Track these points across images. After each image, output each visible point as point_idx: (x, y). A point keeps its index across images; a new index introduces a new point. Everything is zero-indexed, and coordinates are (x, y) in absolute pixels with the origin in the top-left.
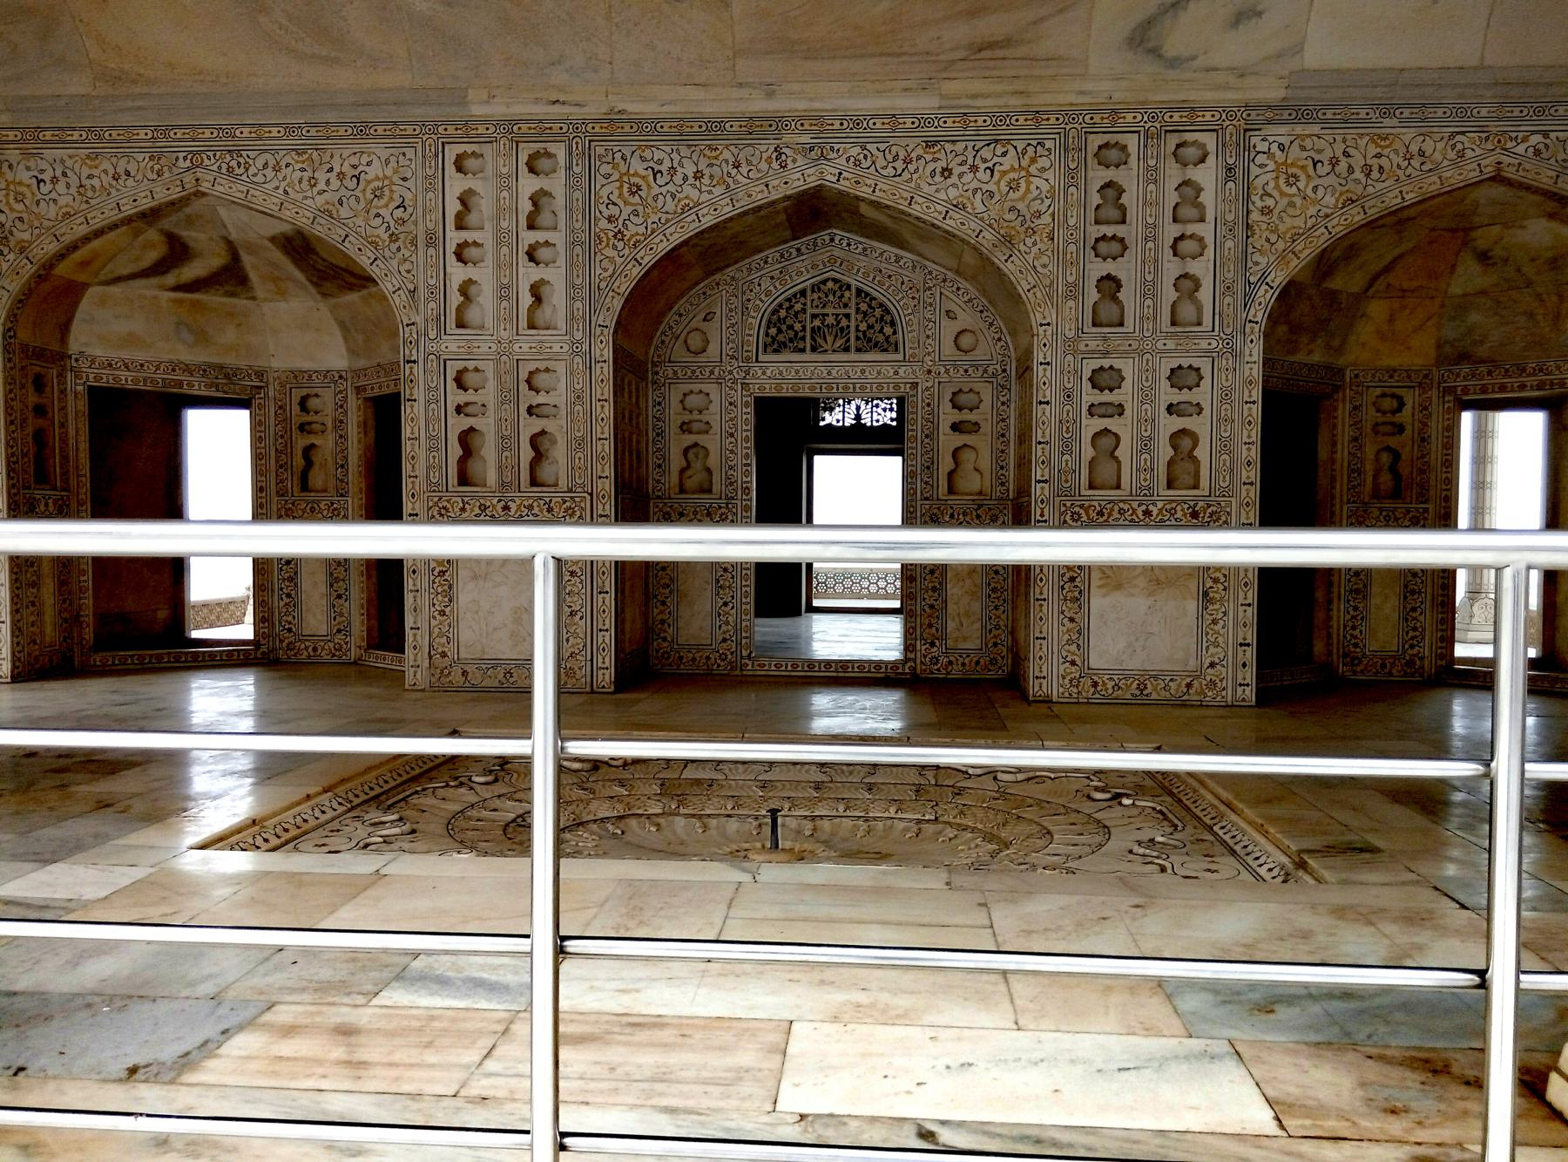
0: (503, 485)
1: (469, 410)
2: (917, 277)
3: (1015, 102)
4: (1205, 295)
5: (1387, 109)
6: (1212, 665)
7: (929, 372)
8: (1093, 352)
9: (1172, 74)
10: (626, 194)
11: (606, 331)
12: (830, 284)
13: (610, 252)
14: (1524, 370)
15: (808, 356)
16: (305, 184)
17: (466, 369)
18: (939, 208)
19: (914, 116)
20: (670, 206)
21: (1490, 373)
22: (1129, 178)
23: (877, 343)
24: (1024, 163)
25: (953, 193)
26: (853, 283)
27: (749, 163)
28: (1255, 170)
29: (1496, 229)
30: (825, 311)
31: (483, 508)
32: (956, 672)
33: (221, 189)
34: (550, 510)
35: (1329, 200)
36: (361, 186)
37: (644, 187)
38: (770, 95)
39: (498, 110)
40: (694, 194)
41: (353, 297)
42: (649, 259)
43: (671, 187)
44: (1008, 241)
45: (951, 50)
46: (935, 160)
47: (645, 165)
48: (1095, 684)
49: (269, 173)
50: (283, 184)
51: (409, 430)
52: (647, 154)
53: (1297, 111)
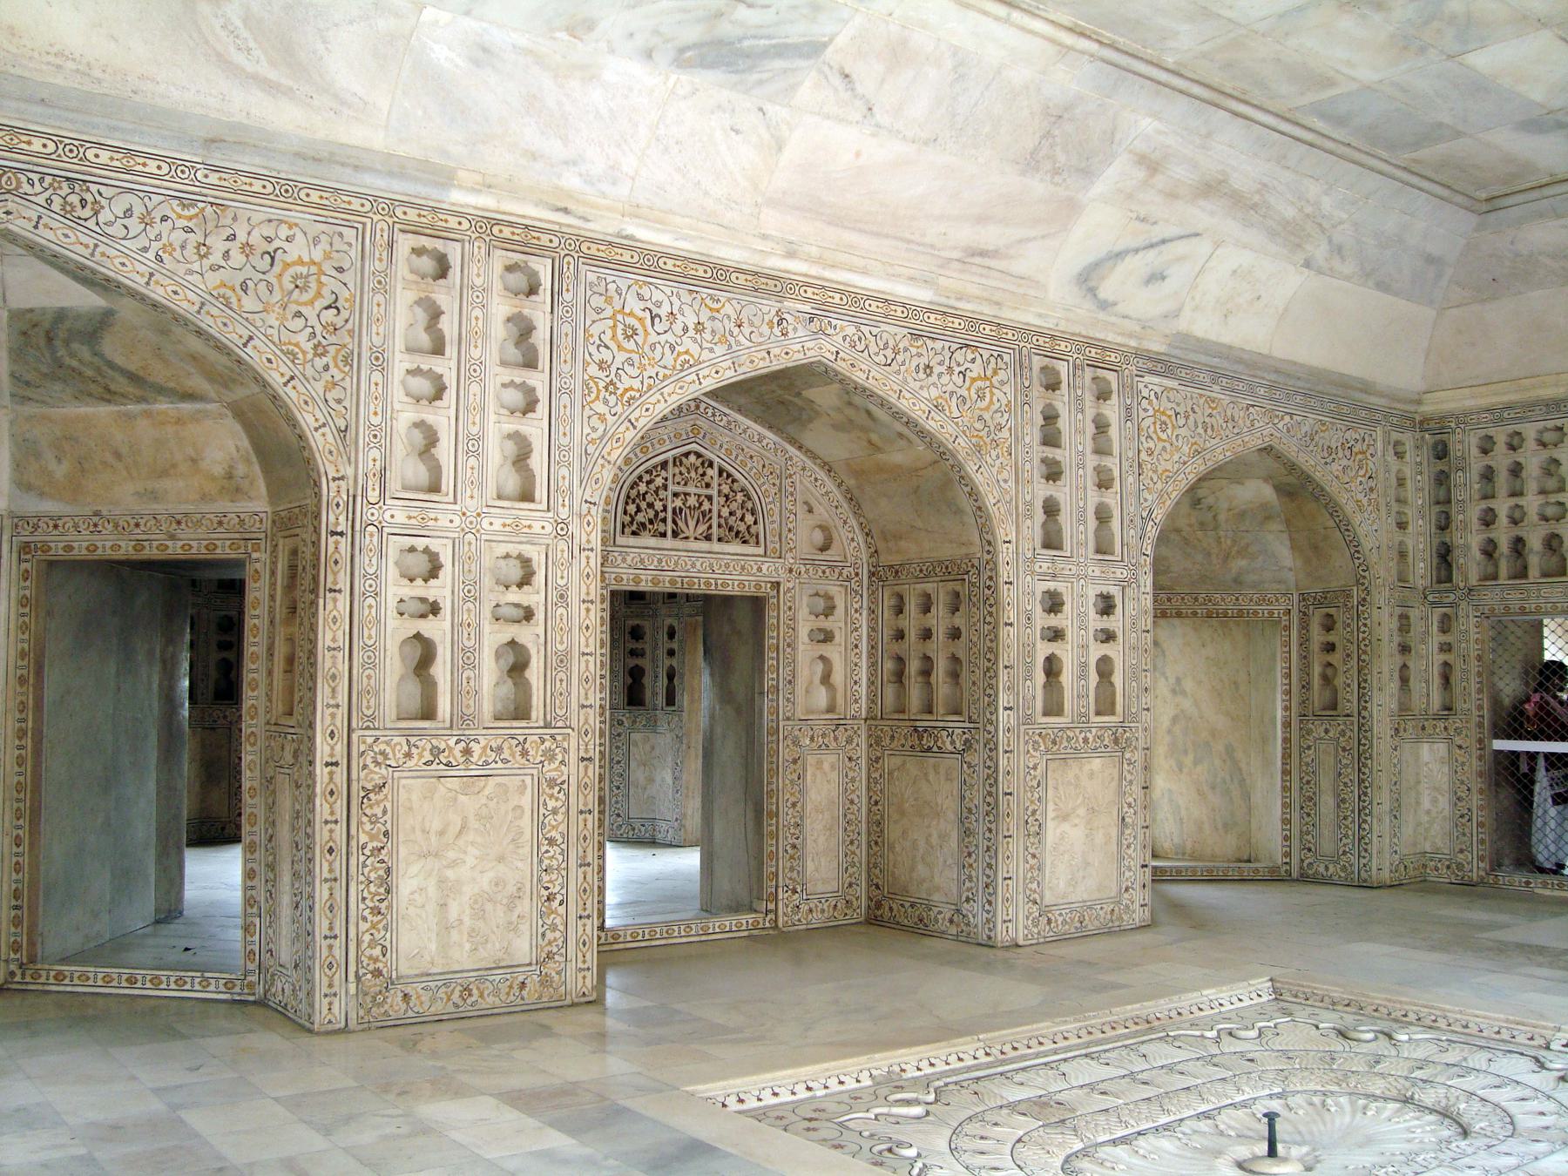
0: (462, 719)
1: (423, 608)
3: (988, 311)
4: (1115, 524)
5: (1216, 375)
6: (1127, 890)
7: (791, 571)
9: (1101, 315)
10: (620, 337)
11: (594, 509)
12: (692, 458)
13: (600, 407)
14: (1196, 599)
15: (669, 542)
16: (190, 251)
17: (412, 549)
19: (904, 305)
20: (669, 359)
21: (1169, 600)
22: (1062, 402)
23: (738, 533)
24: (989, 373)
25: (934, 393)
27: (751, 324)
30: (689, 489)
31: (436, 752)
32: (817, 919)
33: (49, 235)
34: (524, 753)
35: (1186, 449)
38: (791, 255)
39: (486, 201)
40: (695, 350)
41: (104, 410)
42: (644, 422)
43: (669, 337)
44: (978, 449)
45: (955, 248)
46: (919, 355)
47: (642, 305)
49: (135, 225)
51: (329, 635)
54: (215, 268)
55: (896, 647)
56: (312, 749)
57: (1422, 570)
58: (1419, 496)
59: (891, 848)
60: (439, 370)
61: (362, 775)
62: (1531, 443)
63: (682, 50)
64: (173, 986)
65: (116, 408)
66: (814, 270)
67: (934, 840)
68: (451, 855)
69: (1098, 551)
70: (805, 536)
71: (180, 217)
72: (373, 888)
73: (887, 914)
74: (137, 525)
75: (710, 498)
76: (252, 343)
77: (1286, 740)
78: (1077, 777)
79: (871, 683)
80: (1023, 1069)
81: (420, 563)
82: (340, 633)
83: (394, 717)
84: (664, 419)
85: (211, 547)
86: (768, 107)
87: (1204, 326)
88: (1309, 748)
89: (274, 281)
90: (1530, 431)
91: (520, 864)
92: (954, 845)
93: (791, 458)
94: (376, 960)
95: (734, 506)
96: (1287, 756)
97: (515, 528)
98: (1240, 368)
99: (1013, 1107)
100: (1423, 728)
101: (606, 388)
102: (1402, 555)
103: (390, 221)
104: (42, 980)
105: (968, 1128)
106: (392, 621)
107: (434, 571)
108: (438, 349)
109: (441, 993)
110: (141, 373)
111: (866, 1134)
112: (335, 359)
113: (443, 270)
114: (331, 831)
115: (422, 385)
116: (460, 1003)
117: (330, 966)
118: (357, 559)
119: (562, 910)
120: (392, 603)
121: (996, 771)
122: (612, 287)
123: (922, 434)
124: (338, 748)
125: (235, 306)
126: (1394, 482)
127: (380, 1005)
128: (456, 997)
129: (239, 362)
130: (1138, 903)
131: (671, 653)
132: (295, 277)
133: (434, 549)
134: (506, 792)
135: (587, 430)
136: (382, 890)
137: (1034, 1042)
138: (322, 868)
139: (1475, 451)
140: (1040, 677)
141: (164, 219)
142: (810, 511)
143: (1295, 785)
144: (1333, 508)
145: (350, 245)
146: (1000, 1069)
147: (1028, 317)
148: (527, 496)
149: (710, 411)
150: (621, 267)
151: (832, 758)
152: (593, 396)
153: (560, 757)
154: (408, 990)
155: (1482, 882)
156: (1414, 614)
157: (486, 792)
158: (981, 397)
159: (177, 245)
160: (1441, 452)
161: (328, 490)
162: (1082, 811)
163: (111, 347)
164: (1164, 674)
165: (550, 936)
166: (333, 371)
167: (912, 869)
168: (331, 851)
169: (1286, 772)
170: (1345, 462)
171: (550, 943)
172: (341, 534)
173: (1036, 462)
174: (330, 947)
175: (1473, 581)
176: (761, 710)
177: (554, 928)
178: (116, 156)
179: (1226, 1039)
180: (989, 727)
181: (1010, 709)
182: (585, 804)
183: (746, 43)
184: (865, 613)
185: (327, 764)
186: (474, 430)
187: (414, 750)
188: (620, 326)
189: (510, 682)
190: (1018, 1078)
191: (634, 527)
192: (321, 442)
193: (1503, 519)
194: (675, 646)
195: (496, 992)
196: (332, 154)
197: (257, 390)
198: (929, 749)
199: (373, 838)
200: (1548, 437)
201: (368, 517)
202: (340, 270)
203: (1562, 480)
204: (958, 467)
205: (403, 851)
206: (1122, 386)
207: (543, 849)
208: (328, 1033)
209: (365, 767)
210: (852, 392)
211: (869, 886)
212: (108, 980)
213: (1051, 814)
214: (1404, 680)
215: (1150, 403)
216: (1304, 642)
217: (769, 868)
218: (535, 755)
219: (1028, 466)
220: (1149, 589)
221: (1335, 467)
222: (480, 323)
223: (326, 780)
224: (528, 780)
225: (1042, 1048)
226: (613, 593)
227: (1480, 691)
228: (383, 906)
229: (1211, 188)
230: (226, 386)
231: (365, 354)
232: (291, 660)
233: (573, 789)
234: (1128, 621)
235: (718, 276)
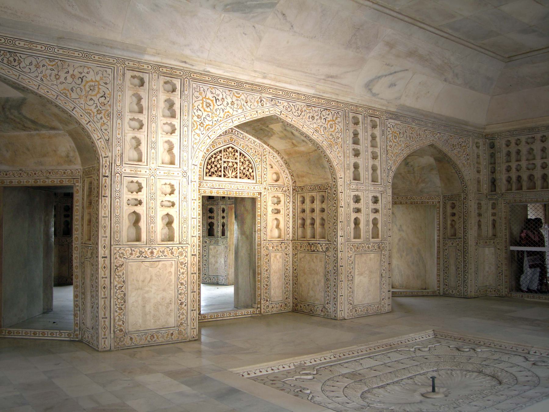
2: (260, 150)
3: (334, 97)
4: (379, 172)
5: (414, 119)
6: (383, 299)
7: (265, 188)
8: (354, 189)
10: (205, 107)
12: (230, 149)
13: (197, 131)
14: (407, 198)
15: (222, 179)
16: (53, 77)
17: (132, 182)
18: (311, 131)
19: (304, 95)
20: (222, 115)
21: (397, 198)
22: (360, 129)
23: (246, 175)
24: (334, 119)
25: (315, 126)
26: (239, 150)
27: (251, 102)
28: (388, 133)
29: (416, 157)
31: (141, 253)
32: (275, 310)
34: (172, 253)
35: (403, 145)
36: (84, 83)
37: (212, 105)
38: (265, 78)
40: (231, 111)
41: (23, 133)
42: (214, 137)
43: (222, 106)
46: (310, 113)
47: (212, 95)
48: (356, 311)
49: (33, 68)
50: (41, 75)
51: (103, 212)
52: (213, 91)
53: (395, 116)
54: (61, 83)
55: (302, 215)
56: (97, 252)
57: (485, 187)
58: (484, 161)
59: (301, 285)
60: (141, 119)
61: (115, 261)
62: (523, 143)
63: (226, 5)
64: (49, 335)
65: (27, 133)
66: (273, 83)
67: (316, 282)
68: (147, 289)
69: (373, 181)
70: (270, 177)
71: (49, 65)
72: (119, 301)
73: (299, 308)
74: (35, 174)
75: (237, 163)
76: (75, 109)
77: (438, 247)
78: (365, 260)
79: (293, 228)
80: (347, 362)
81: (135, 187)
82: (107, 211)
83: (126, 241)
84: (220, 135)
85: (61, 181)
86: (256, 26)
87: (409, 102)
88: (446, 250)
89: (82, 87)
90: (523, 138)
91: (171, 292)
92: (323, 284)
93: (265, 149)
94: (121, 326)
95: (245, 166)
96: (438, 252)
97: (168, 174)
98: (422, 117)
99: (343, 375)
100: (486, 243)
101: (200, 125)
102: (479, 182)
103: (123, 66)
104: (3, 334)
105: (328, 383)
106: (125, 207)
107: (140, 189)
108: (141, 112)
109: (143, 337)
110: (36, 120)
111: (292, 385)
112: (104, 115)
113: (142, 83)
114: (104, 281)
115: (136, 124)
116: (150, 340)
117: (105, 328)
118: (113, 185)
119: (185, 308)
120: (125, 201)
121: (337, 258)
122: (202, 89)
123: (311, 140)
124: (107, 252)
125: (69, 97)
126: (476, 156)
127: (122, 342)
128: (149, 339)
129: (71, 116)
130: (387, 305)
131: (223, 217)
132: (90, 86)
133: (140, 181)
134: (166, 267)
135: (193, 139)
136: (122, 301)
137: (351, 353)
138: (101, 294)
139: (504, 146)
140: (353, 225)
141: (43, 66)
142: (272, 167)
143: (442, 263)
144: (455, 166)
145: (109, 75)
146: (339, 362)
147: (348, 99)
148: (172, 163)
149: (236, 133)
150: (205, 82)
151: (280, 254)
152: (195, 127)
153: (184, 255)
154: (132, 336)
155: (506, 296)
156: (483, 203)
157: (159, 267)
158: (331, 127)
159: (48, 75)
160: (492, 146)
161: (102, 161)
162: (367, 272)
163: (25, 111)
164: (396, 224)
165: (181, 317)
166: (104, 119)
167: (308, 293)
168: (104, 288)
169: (438, 258)
170: (459, 150)
171: (181, 319)
172: (107, 176)
173: (351, 150)
174: (105, 321)
175: (503, 191)
176: (255, 238)
177: (183, 314)
178: (26, 43)
179: (417, 351)
180: (335, 243)
181: (342, 236)
182: (194, 271)
183: (248, 3)
184: (291, 203)
185: (103, 257)
186: (154, 140)
187: (133, 252)
188: (205, 103)
189: (167, 228)
190: (346, 365)
191: (210, 174)
192: (100, 144)
193: (514, 169)
194: (225, 215)
195: (163, 337)
196: (102, 43)
197: (77, 126)
198: (314, 251)
199: (119, 283)
200: (529, 141)
201: (116, 171)
202: (106, 84)
203: (534, 156)
204: (324, 152)
205: (130, 288)
206: (381, 123)
207: (179, 286)
208: (104, 351)
209: (116, 258)
210: (286, 126)
211: (293, 299)
212: (26, 333)
213: (356, 273)
214: (479, 226)
215: (391, 129)
216: (445, 212)
217: (258, 293)
218: (176, 253)
219: (348, 151)
220: (390, 194)
221: (455, 151)
222: (155, 102)
223: (103, 262)
224: (173, 262)
225: (354, 355)
226: (203, 197)
227: (506, 229)
228: (123, 307)
229: (411, 54)
230: (66, 125)
231: (115, 113)
232: (90, 221)
233: (189, 265)
234: (383, 205)
235: (239, 85)
